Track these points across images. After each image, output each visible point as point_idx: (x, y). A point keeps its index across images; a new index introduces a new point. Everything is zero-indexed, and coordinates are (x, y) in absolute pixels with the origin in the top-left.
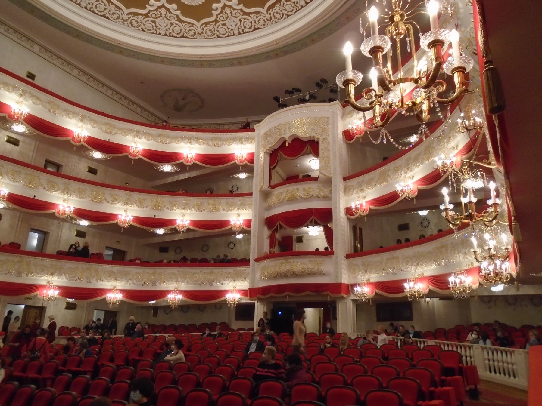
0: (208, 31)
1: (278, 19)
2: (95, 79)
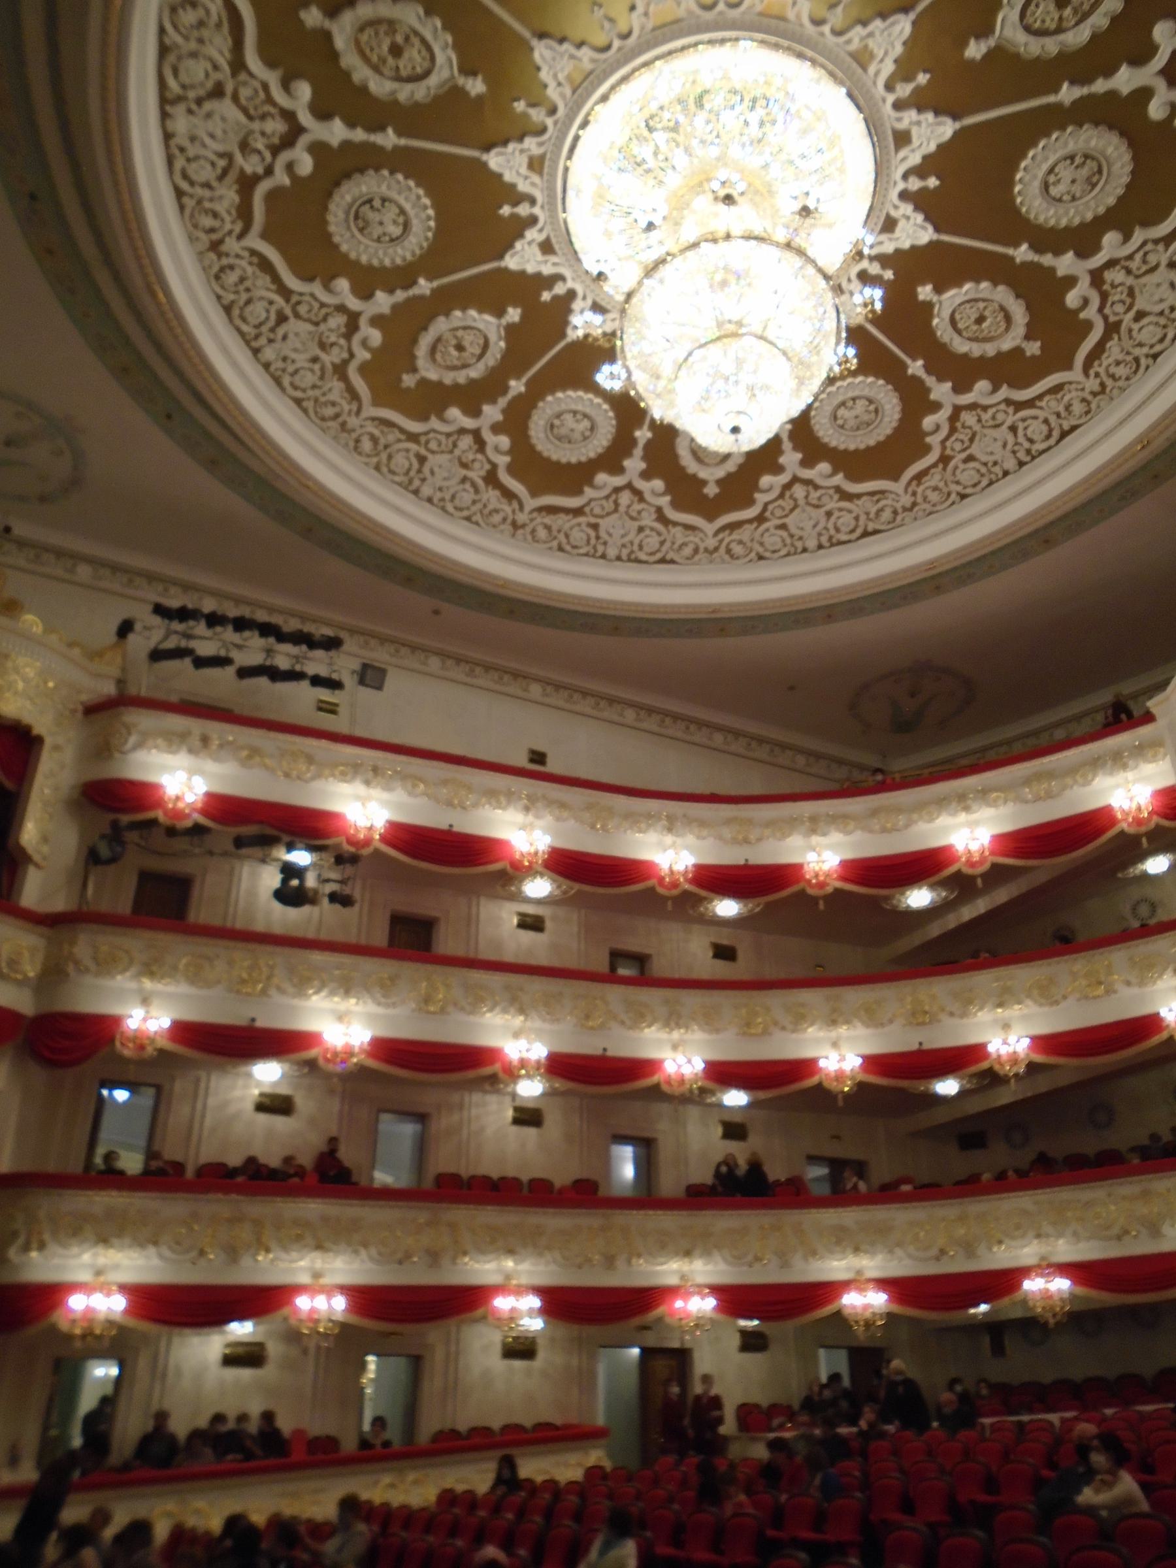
0: (929, 493)
1: (1127, 379)
2: (676, 717)
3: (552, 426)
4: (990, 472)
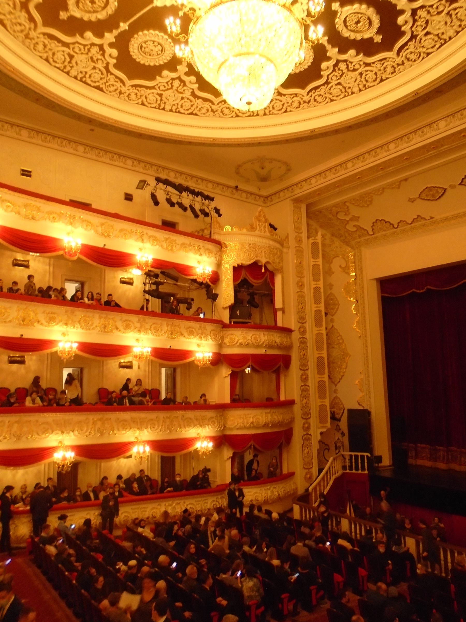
3: (141, 47)
4: (346, 91)
